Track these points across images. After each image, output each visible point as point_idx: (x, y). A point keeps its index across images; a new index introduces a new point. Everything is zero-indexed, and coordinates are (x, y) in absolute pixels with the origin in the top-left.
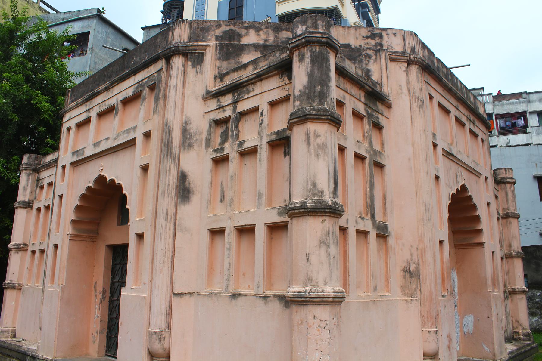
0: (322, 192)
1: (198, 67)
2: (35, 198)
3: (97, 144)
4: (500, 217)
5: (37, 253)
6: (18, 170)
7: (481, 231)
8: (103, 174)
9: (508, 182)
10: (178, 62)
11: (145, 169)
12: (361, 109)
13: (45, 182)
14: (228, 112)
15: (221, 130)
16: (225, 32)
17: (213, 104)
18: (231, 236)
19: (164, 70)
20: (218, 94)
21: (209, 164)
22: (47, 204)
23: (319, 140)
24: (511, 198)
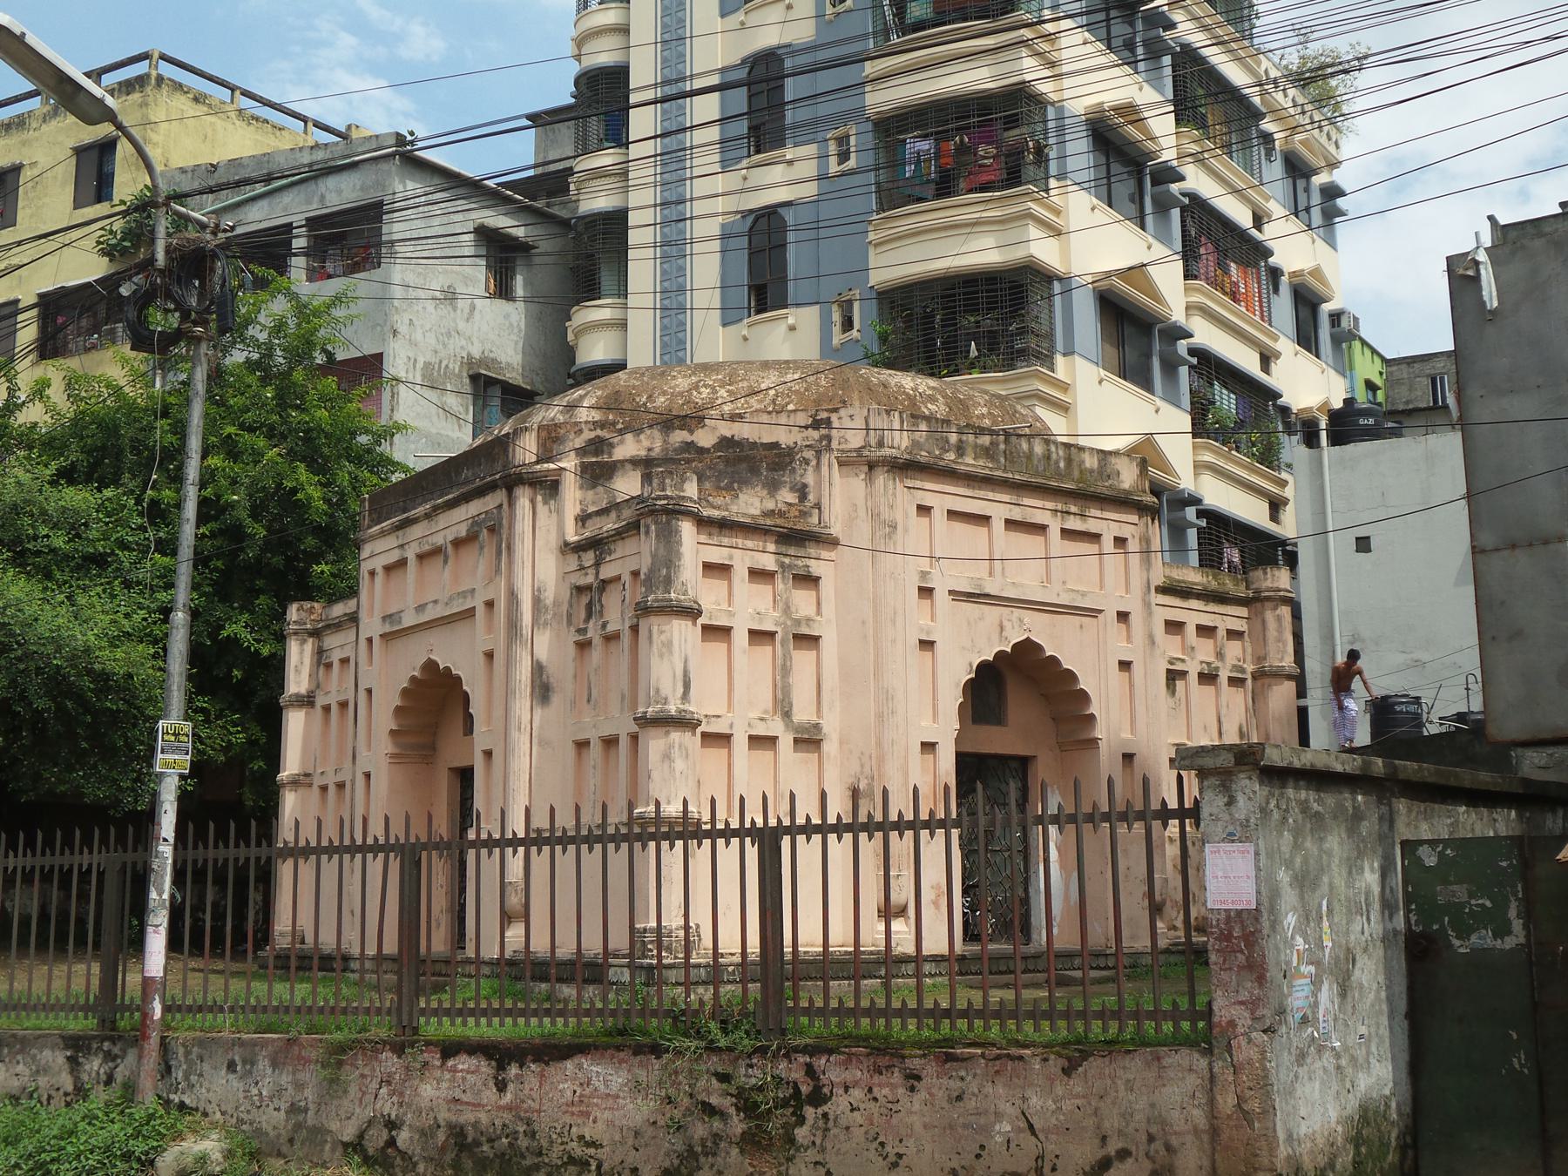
0: (666, 699)
1: (552, 502)
2: (318, 686)
3: (420, 608)
4: (1249, 676)
5: (332, 789)
6: (281, 638)
7: (1092, 717)
8: (433, 657)
9: (1268, 599)
11: (490, 655)
12: (768, 562)
13: (335, 657)
14: (590, 579)
15: (585, 600)
17: (572, 561)
18: (596, 750)
19: (505, 506)
20: (579, 548)
21: (571, 650)
22: (342, 698)
23: (663, 637)
24: (1275, 634)
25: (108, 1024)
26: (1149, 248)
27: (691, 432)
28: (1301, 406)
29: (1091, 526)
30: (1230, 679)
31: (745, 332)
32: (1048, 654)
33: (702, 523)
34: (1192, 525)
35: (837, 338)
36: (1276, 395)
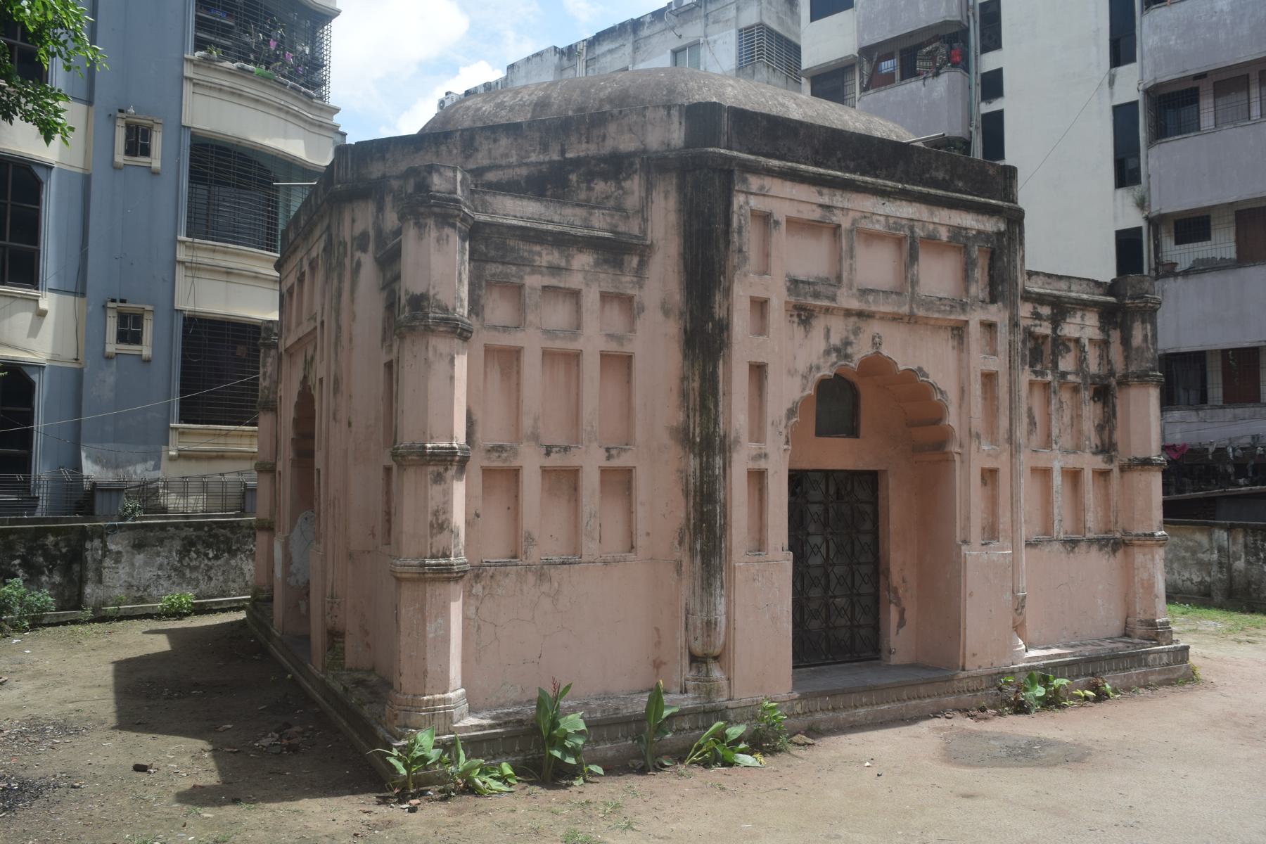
14: (1045, 329)
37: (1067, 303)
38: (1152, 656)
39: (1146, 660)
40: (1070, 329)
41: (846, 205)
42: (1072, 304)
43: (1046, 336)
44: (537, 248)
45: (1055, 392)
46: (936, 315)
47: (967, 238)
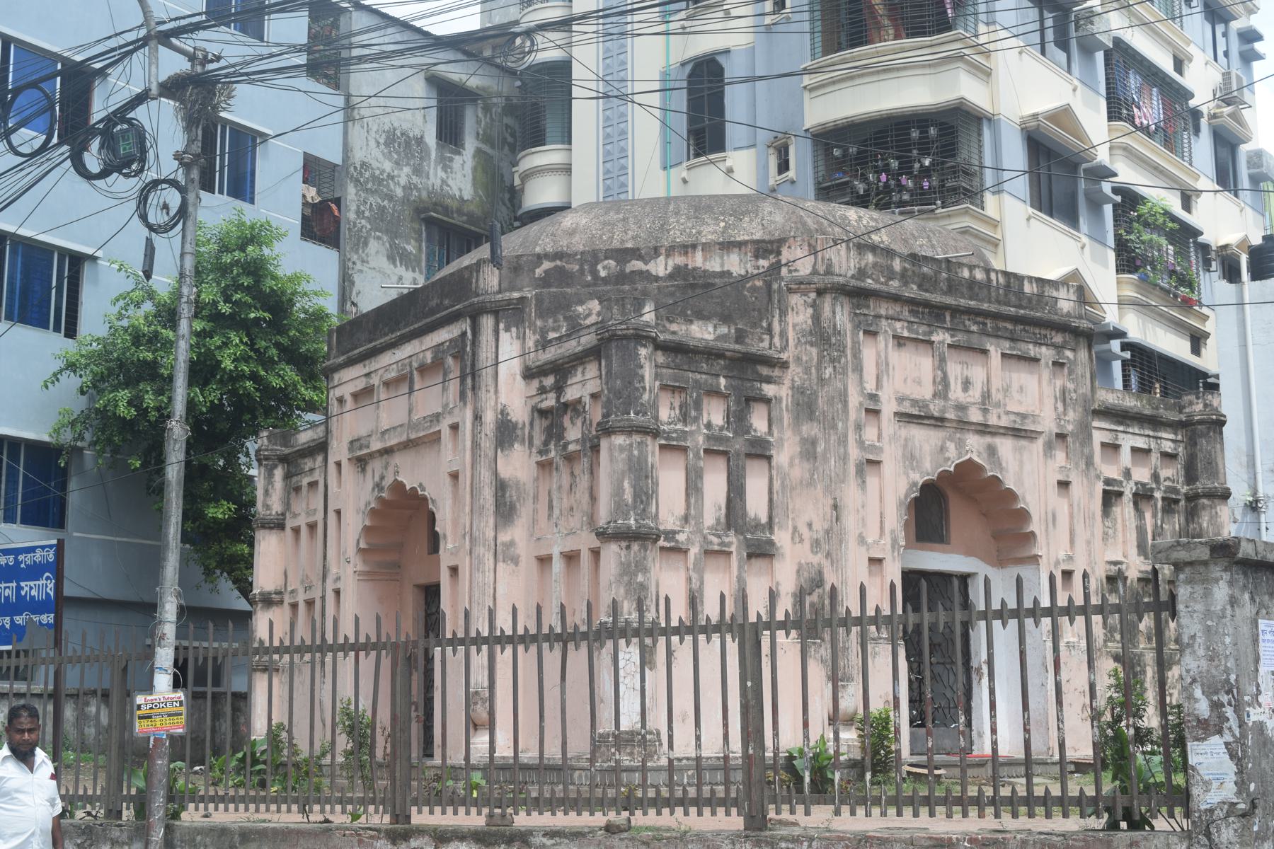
7: (1033, 533)
8: (399, 479)
10: (487, 322)
11: (455, 476)
14: (550, 401)
16: (546, 272)
17: (535, 383)
18: (558, 565)
21: (534, 469)
22: (311, 519)
25: (114, 812)
26: (1074, 90)
27: (646, 264)
28: (1221, 243)
29: (1032, 350)
30: (1163, 499)
31: (684, 174)
32: (990, 474)
33: (659, 346)
34: (1117, 357)
35: (773, 178)
36: (1196, 233)
37: (563, 364)
38: (577, 774)
39: (572, 776)
40: (571, 394)
41: (377, 367)
42: (568, 363)
43: (552, 407)
44: (306, 460)
45: (557, 469)
46: (422, 434)
47: (443, 352)
